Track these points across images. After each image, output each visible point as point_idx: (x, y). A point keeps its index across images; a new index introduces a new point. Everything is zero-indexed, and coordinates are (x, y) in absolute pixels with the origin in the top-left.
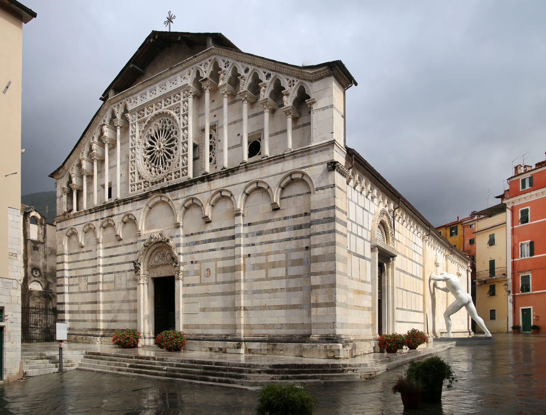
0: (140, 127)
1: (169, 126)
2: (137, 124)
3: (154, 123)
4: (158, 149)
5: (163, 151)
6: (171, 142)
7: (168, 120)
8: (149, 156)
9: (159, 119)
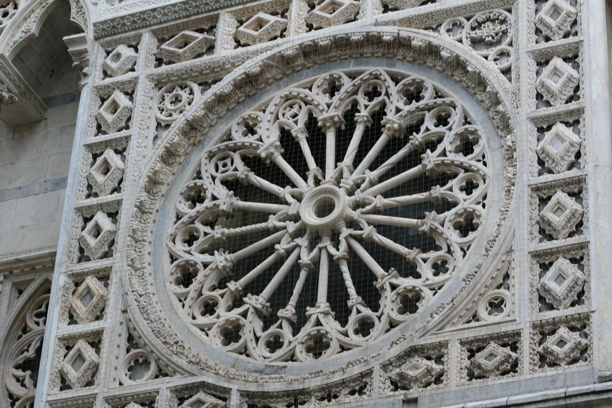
0: (167, 104)
1: (406, 108)
2: (144, 88)
3: (285, 92)
4: (310, 218)
5: (345, 232)
6: (427, 189)
7: (396, 79)
8: (221, 259)
9: (326, 75)
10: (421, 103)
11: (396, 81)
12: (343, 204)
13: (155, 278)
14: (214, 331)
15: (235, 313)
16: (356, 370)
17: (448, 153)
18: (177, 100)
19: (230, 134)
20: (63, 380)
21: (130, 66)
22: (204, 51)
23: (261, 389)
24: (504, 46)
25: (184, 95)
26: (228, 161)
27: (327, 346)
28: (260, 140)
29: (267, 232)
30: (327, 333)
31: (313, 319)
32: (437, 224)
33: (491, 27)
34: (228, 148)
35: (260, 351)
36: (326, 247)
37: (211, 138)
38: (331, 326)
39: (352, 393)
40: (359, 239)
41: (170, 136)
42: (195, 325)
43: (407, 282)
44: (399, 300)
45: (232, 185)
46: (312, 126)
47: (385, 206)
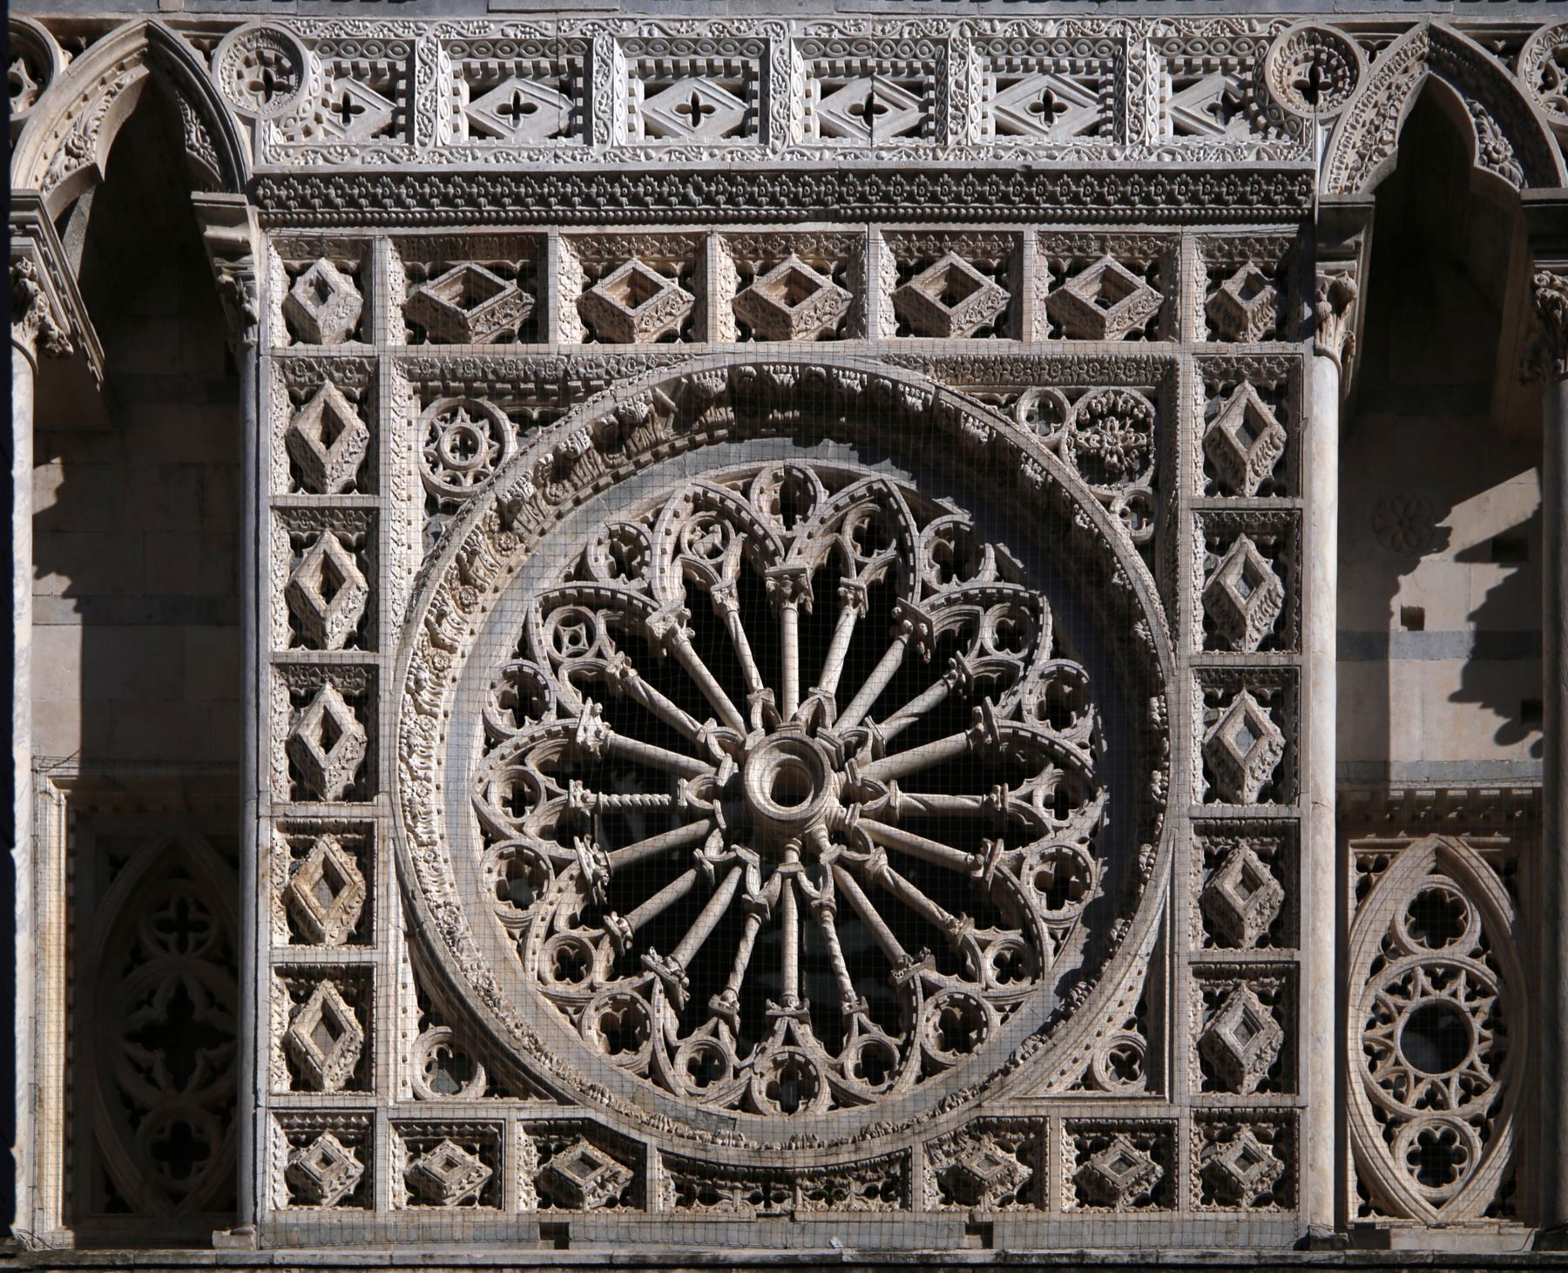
10: (972, 585)
13: (456, 872)
14: (592, 1020)
15: (626, 986)
18: (467, 445)
22: (516, 328)
27: (810, 1093)
28: (648, 592)
30: (808, 1062)
31: (781, 1026)
34: (581, 599)
36: (794, 876)
40: (857, 871)
42: (546, 995)
45: (592, 685)
46: (749, 581)
47: (907, 808)
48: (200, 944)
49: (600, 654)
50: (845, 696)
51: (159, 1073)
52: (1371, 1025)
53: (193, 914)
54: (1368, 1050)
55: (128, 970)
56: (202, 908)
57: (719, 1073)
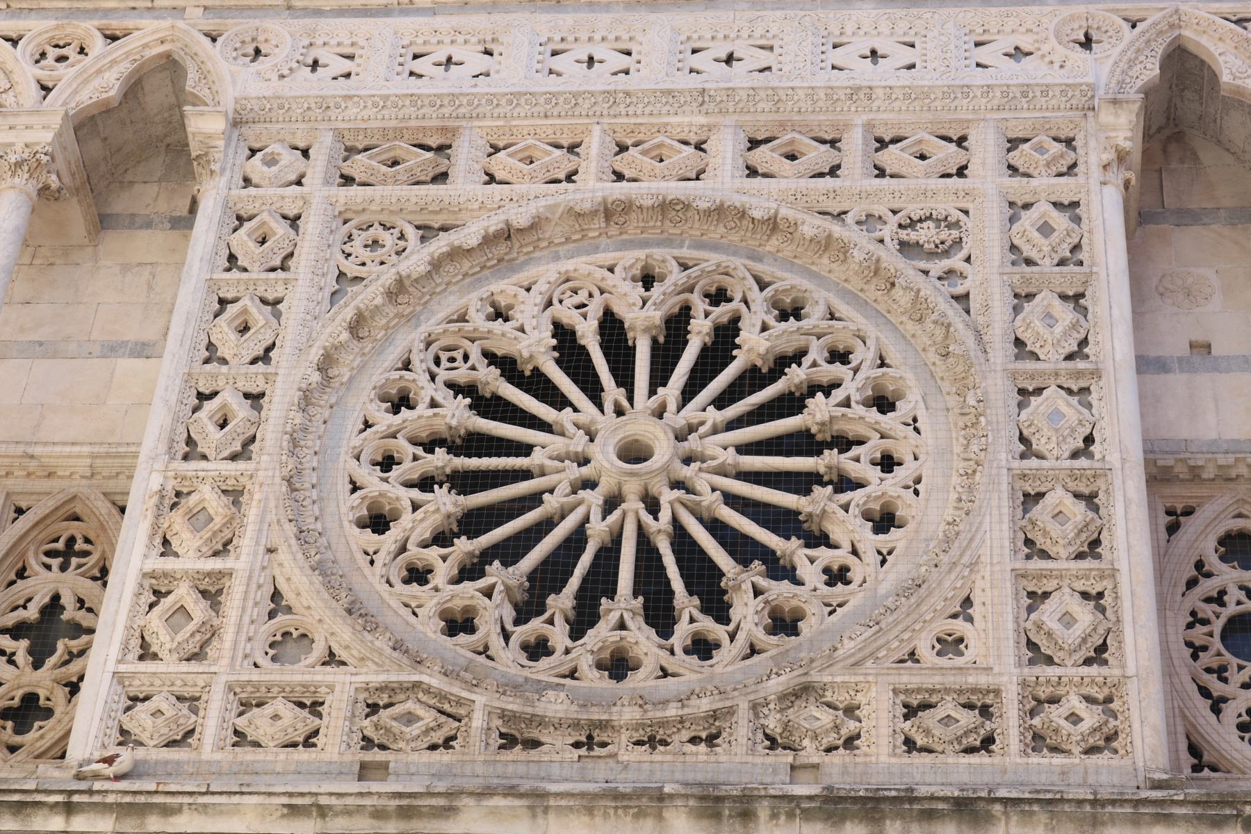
8: (445, 502)
9: (641, 254)
11: (763, 286)
12: (663, 450)
16: (704, 705)
17: (853, 404)
19: (465, 314)
20: (144, 645)
21: (293, 177)
23: (529, 710)
24: (956, 262)
25: (388, 239)
26: (458, 355)
29: (526, 475)
32: (833, 507)
33: (933, 231)
35: (509, 659)
37: (433, 313)
38: (642, 639)
39: (694, 740)
41: (369, 295)
43: (780, 590)
44: (766, 612)
46: (611, 327)
48: (79, 566)
49: (473, 368)
50: (688, 393)
51: (22, 658)
52: (1190, 626)
53: (80, 545)
54: (1189, 644)
55: (12, 583)
56: (87, 541)
57: (549, 652)
